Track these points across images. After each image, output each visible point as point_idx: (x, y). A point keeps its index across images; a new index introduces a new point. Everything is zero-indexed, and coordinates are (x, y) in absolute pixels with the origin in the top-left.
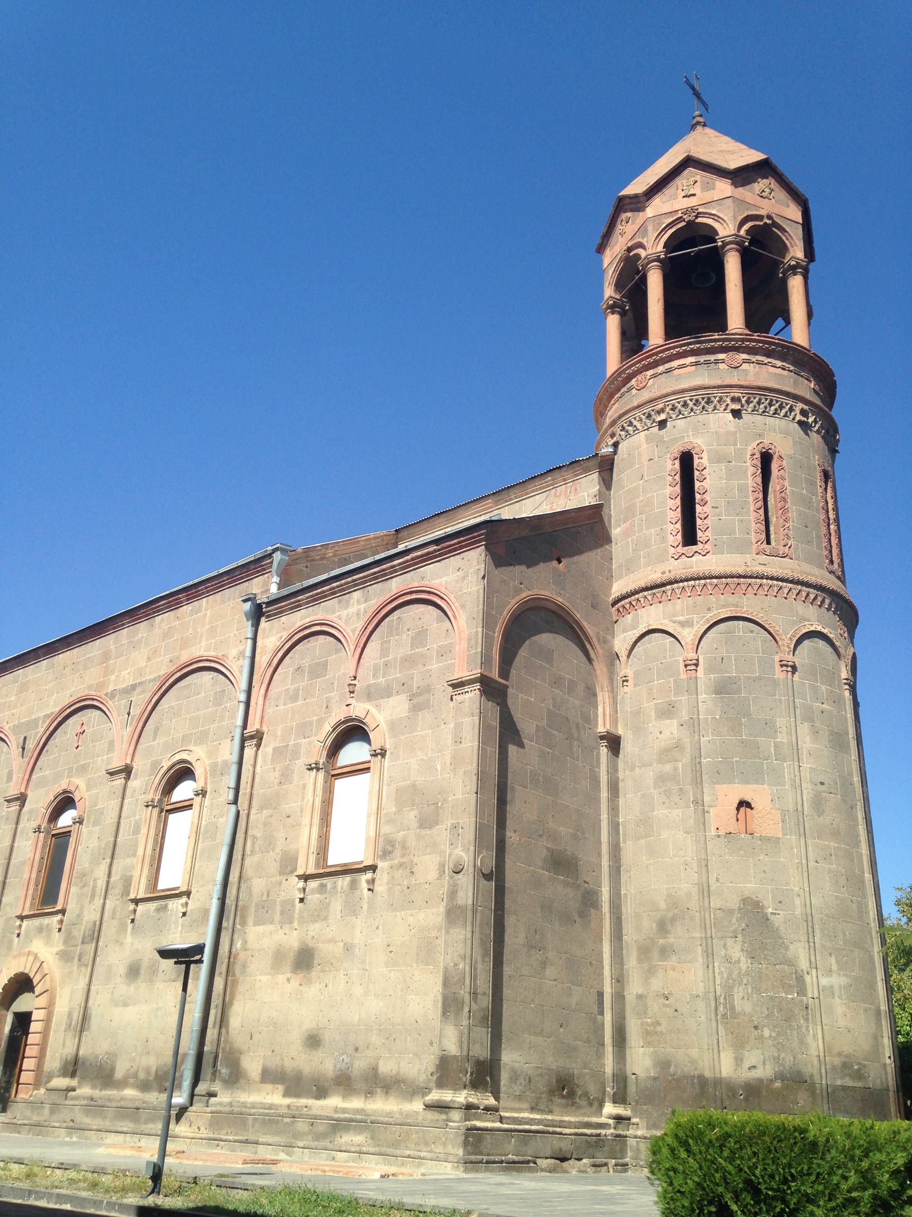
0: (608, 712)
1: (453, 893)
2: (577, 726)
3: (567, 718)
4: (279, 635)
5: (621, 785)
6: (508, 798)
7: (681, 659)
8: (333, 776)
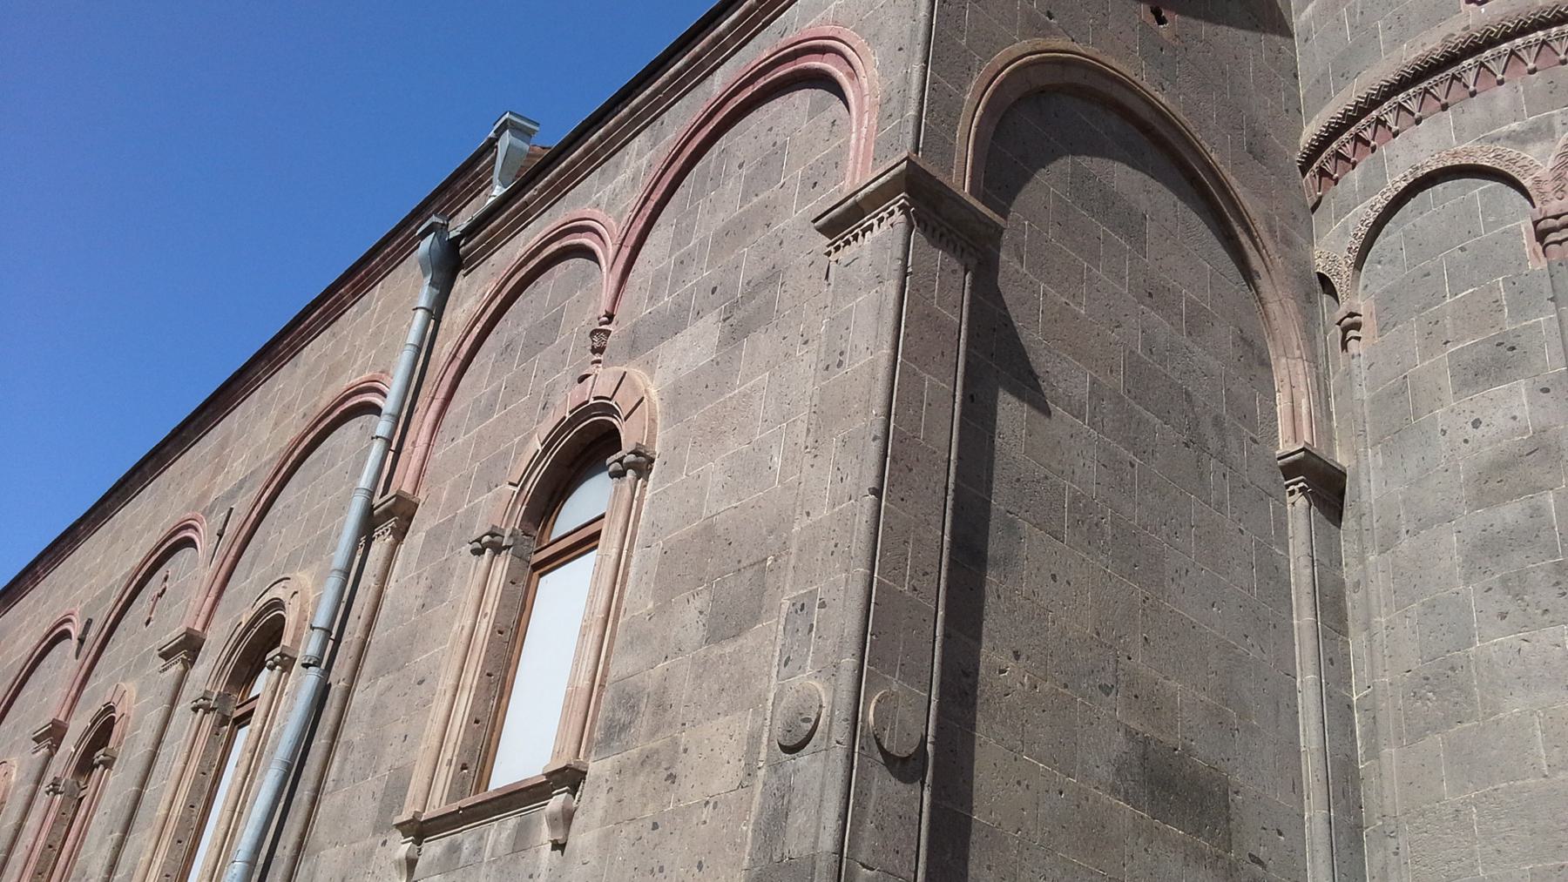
0: (1304, 410)
1: (774, 822)
2: (1217, 422)
3: (1187, 393)
4: (481, 291)
5: (1352, 599)
6: (994, 548)
7: (1526, 226)
8: (536, 567)
